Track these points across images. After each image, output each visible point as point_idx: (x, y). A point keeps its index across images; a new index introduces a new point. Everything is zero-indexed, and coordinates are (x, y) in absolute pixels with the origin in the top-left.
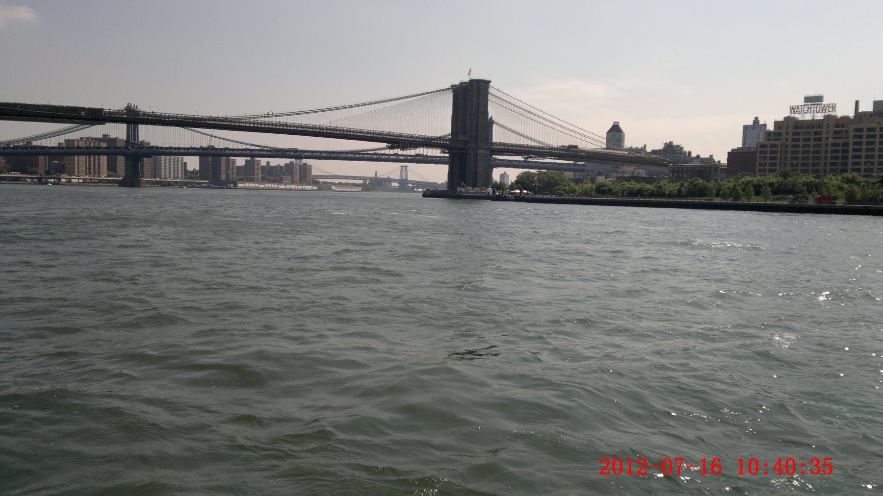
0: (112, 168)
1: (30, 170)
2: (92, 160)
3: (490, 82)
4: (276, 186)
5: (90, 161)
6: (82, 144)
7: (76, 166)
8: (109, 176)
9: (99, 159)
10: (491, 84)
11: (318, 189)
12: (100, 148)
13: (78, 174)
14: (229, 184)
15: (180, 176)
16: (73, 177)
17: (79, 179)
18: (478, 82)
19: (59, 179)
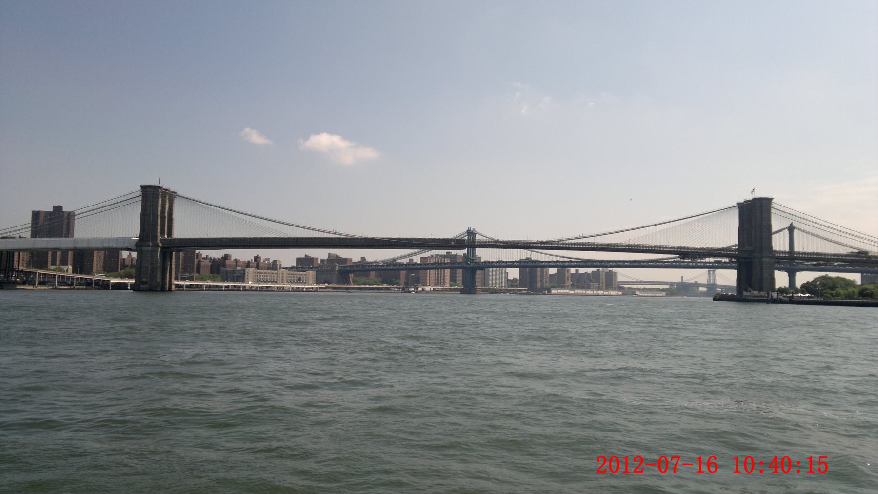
0: (453, 279)
1: (394, 281)
2: (439, 273)
3: (771, 199)
4: (584, 292)
5: (438, 274)
6: (433, 261)
7: (428, 278)
8: (451, 286)
10: (773, 201)
11: (623, 294)
12: (445, 264)
13: (429, 284)
14: (544, 290)
15: (504, 285)
16: (426, 287)
17: (431, 288)
18: (761, 200)
19: (417, 289)
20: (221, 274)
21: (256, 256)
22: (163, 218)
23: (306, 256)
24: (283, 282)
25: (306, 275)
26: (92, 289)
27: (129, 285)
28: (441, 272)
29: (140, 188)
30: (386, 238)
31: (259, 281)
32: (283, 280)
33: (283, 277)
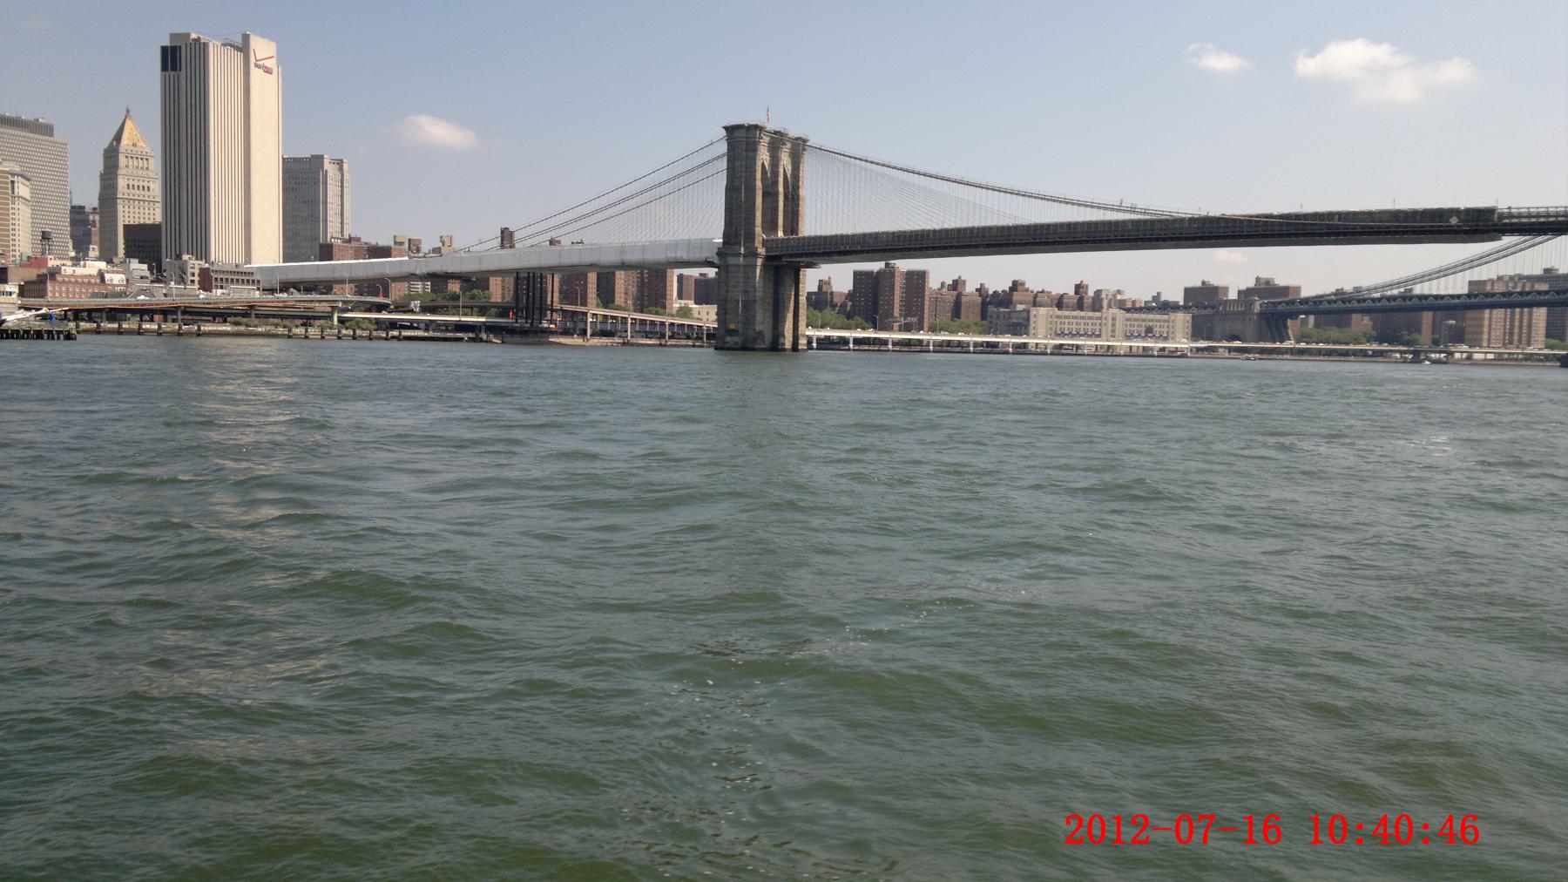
1: (1407, 337)
2: (1517, 317)
5: (1512, 321)
6: (1499, 288)
7: (1486, 330)
9: (1531, 314)
13: (1489, 343)
16: (1477, 349)
17: (1486, 353)
19: (1451, 354)
20: (989, 319)
21: (1078, 282)
22: (770, 194)
23: (1203, 283)
24: (1113, 336)
25: (1168, 321)
26: (702, 347)
27: (815, 341)
28: (1521, 314)
29: (724, 133)
30: (1257, 216)
31: (1062, 335)
32: (1113, 331)
33: (1113, 325)
